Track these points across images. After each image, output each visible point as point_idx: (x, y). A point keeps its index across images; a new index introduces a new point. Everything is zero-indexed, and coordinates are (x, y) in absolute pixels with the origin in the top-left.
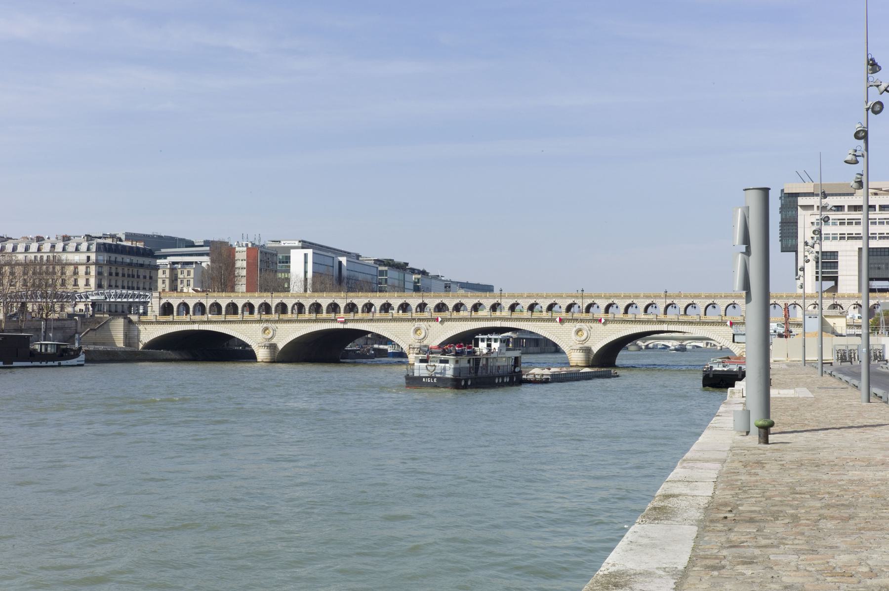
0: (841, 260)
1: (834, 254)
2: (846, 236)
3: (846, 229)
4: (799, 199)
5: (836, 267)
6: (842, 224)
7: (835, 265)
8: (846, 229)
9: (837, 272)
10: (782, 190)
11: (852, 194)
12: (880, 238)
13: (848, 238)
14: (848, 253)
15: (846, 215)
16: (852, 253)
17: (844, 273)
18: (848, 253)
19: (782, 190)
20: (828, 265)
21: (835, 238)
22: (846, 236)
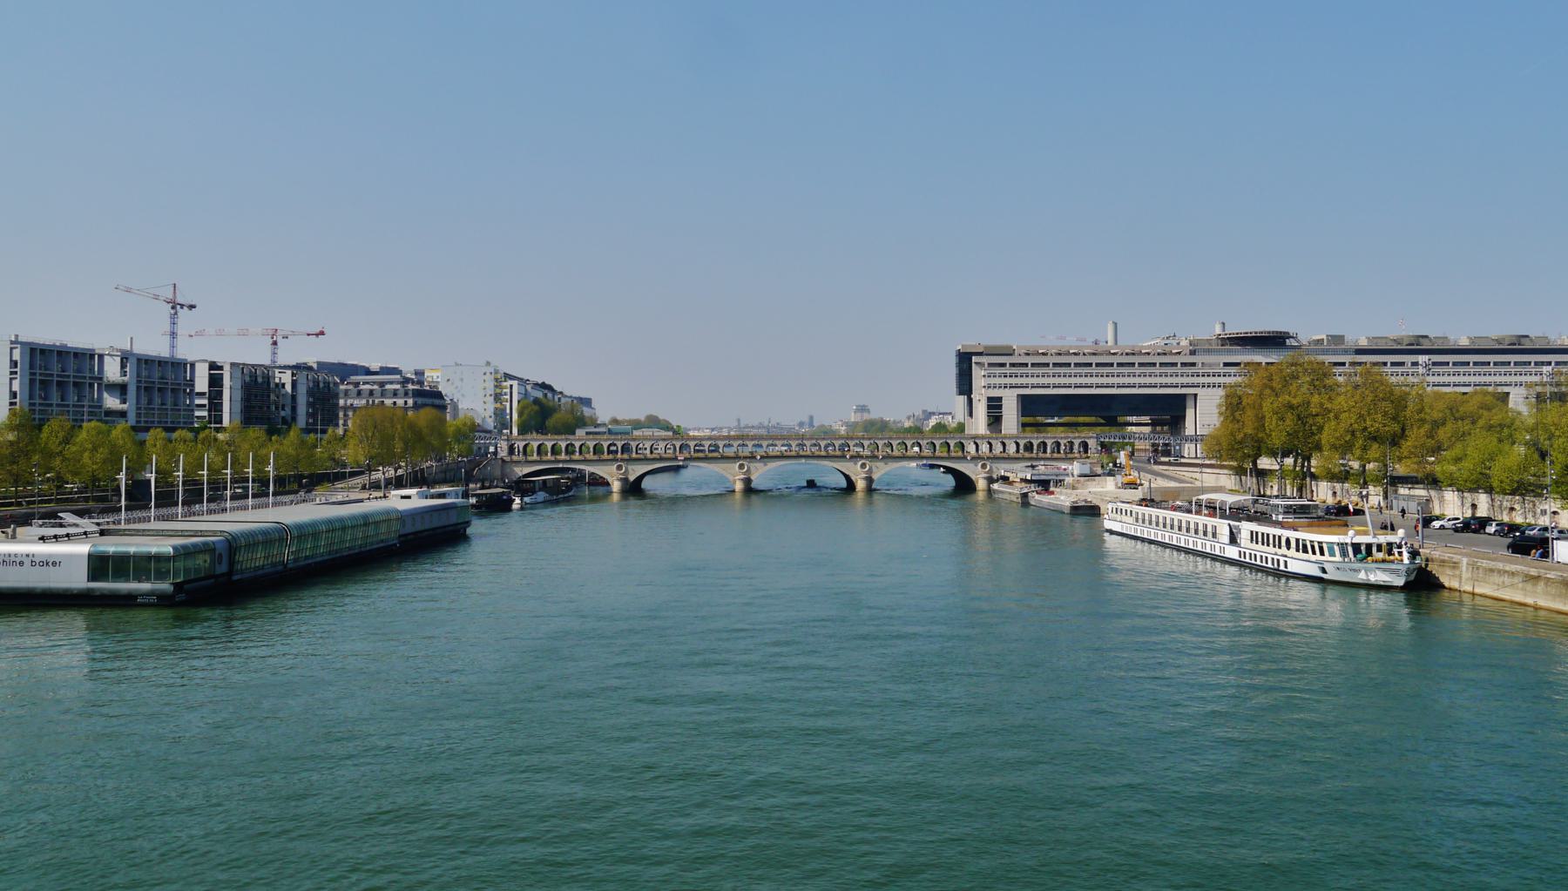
1: (1000, 399)
3: (1008, 381)
7: (1000, 407)
8: (1008, 381)
15: (1008, 370)
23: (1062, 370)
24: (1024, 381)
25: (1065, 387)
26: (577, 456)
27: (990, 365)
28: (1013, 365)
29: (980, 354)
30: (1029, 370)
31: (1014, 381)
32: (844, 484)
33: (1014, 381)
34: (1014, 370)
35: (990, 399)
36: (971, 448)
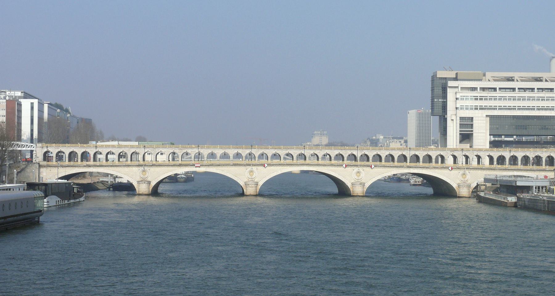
0: (475, 123)
2: (479, 107)
3: (479, 103)
4: (449, 82)
5: (472, 128)
6: (476, 99)
8: (479, 103)
9: (472, 131)
10: (434, 78)
11: (481, 80)
12: (500, 109)
13: (480, 109)
14: (480, 118)
16: (482, 119)
17: (477, 131)
18: (480, 118)
19: (434, 78)
20: (467, 125)
21: (471, 109)
22: (479, 107)
23: (527, 94)
24: (492, 103)
25: (528, 109)
26: (91, 162)
27: (462, 88)
28: (483, 89)
29: (456, 79)
30: (498, 94)
31: (483, 103)
32: (336, 191)
33: (483, 103)
34: (484, 94)
35: (462, 119)
36: (450, 161)
